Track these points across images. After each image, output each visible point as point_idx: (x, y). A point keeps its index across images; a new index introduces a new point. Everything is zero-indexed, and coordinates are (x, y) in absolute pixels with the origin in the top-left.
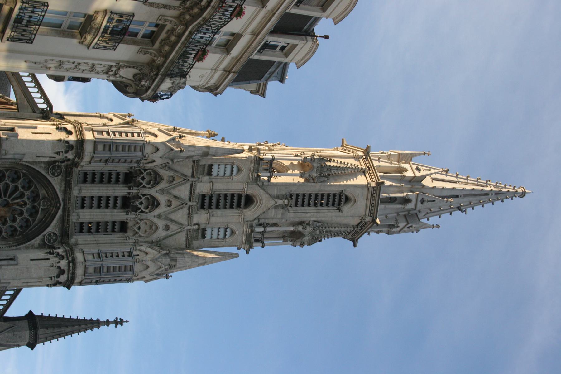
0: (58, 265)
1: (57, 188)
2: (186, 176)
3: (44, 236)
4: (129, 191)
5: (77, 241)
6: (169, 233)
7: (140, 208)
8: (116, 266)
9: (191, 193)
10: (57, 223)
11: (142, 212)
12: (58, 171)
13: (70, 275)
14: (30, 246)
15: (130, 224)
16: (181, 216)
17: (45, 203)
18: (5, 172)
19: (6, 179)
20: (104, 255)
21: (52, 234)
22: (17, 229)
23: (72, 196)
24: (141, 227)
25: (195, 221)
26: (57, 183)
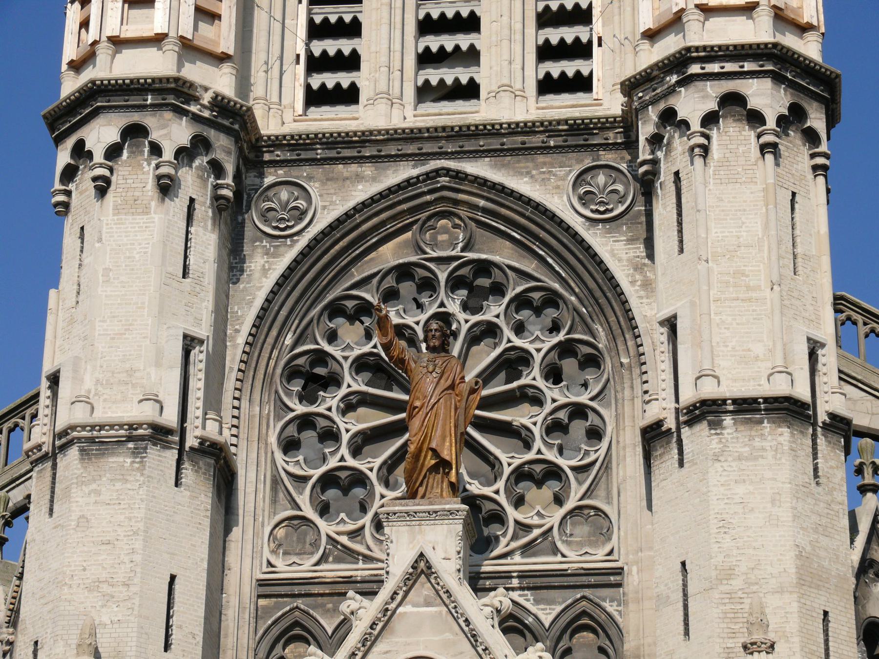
0: (696, 126)
1: (362, 192)
10: (532, 177)
13: (748, 66)
14: (638, 277)
17: (443, 237)
18: (291, 415)
19: (321, 409)
22: (560, 343)
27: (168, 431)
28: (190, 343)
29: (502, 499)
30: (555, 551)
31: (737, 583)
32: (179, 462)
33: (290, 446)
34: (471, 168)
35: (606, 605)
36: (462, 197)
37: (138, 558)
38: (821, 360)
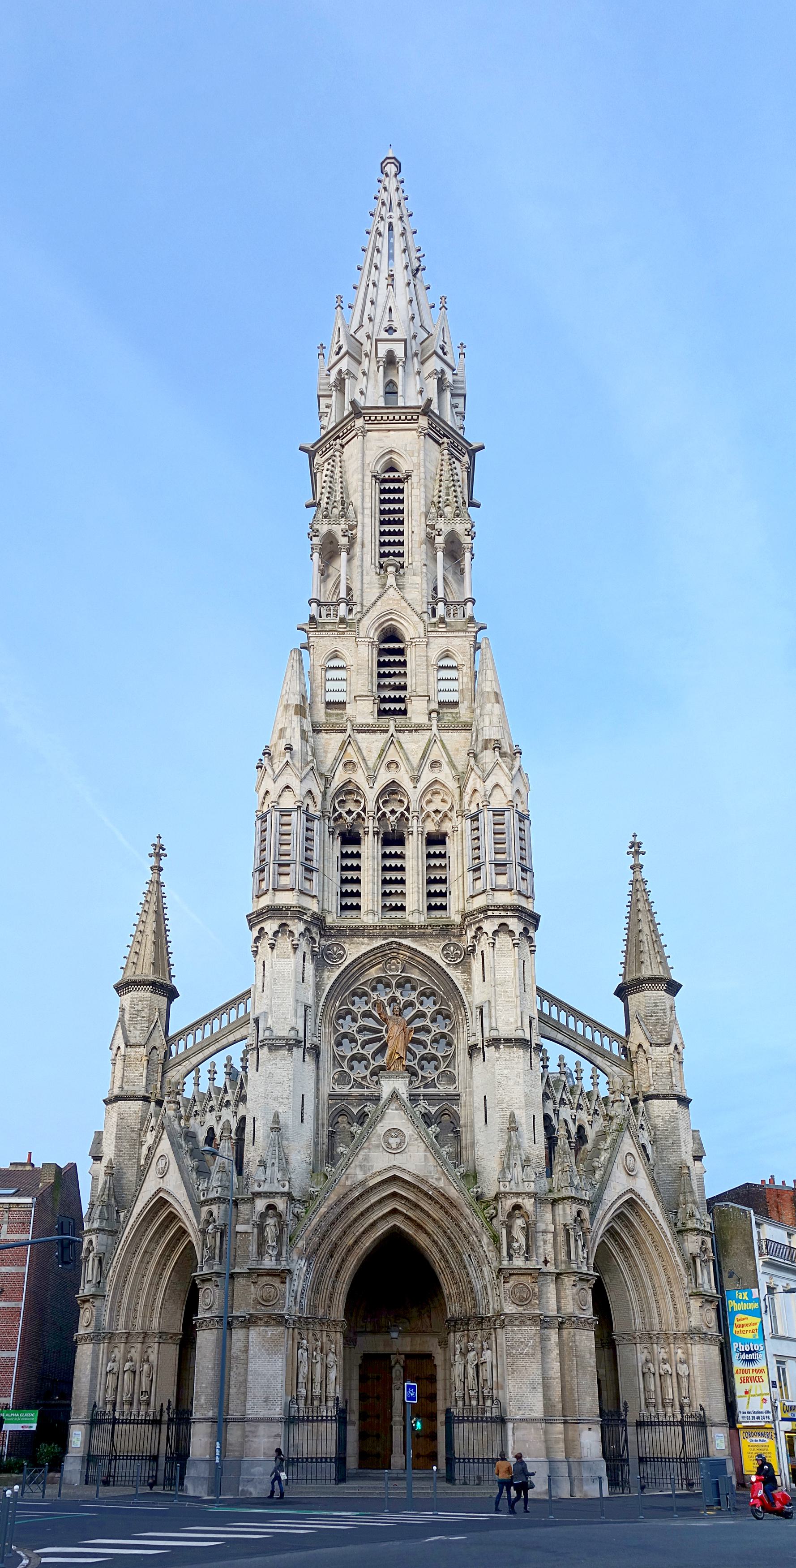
0: (490, 935)
2: (344, 742)
3: (449, 965)
4: (371, 833)
5: (458, 912)
6: (444, 760)
7: (402, 814)
8: (494, 839)
9: (374, 731)
11: (408, 809)
12: (335, 949)
13: (510, 913)
15: (431, 827)
16: (414, 744)
17: (393, 967)
20: (477, 861)
21: (445, 952)
23: (380, 924)
24: (434, 809)
25: (424, 720)
26: (355, 950)
27: (301, 1042)
28: (307, 1007)
29: (416, 1067)
30: (436, 1087)
31: (504, 1105)
32: (304, 1053)
33: (339, 1044)
34: (405, 942)
35: (454, 1107)
36: (401, 952)
37: (291, 1089)
38: (533, 1024)
